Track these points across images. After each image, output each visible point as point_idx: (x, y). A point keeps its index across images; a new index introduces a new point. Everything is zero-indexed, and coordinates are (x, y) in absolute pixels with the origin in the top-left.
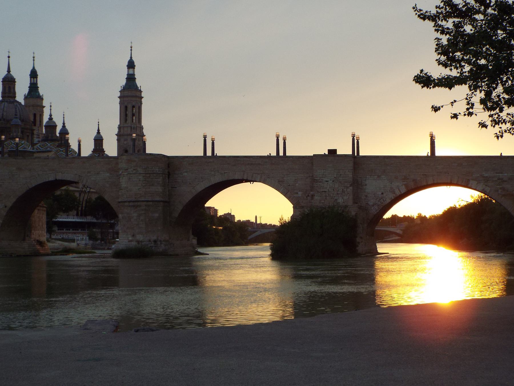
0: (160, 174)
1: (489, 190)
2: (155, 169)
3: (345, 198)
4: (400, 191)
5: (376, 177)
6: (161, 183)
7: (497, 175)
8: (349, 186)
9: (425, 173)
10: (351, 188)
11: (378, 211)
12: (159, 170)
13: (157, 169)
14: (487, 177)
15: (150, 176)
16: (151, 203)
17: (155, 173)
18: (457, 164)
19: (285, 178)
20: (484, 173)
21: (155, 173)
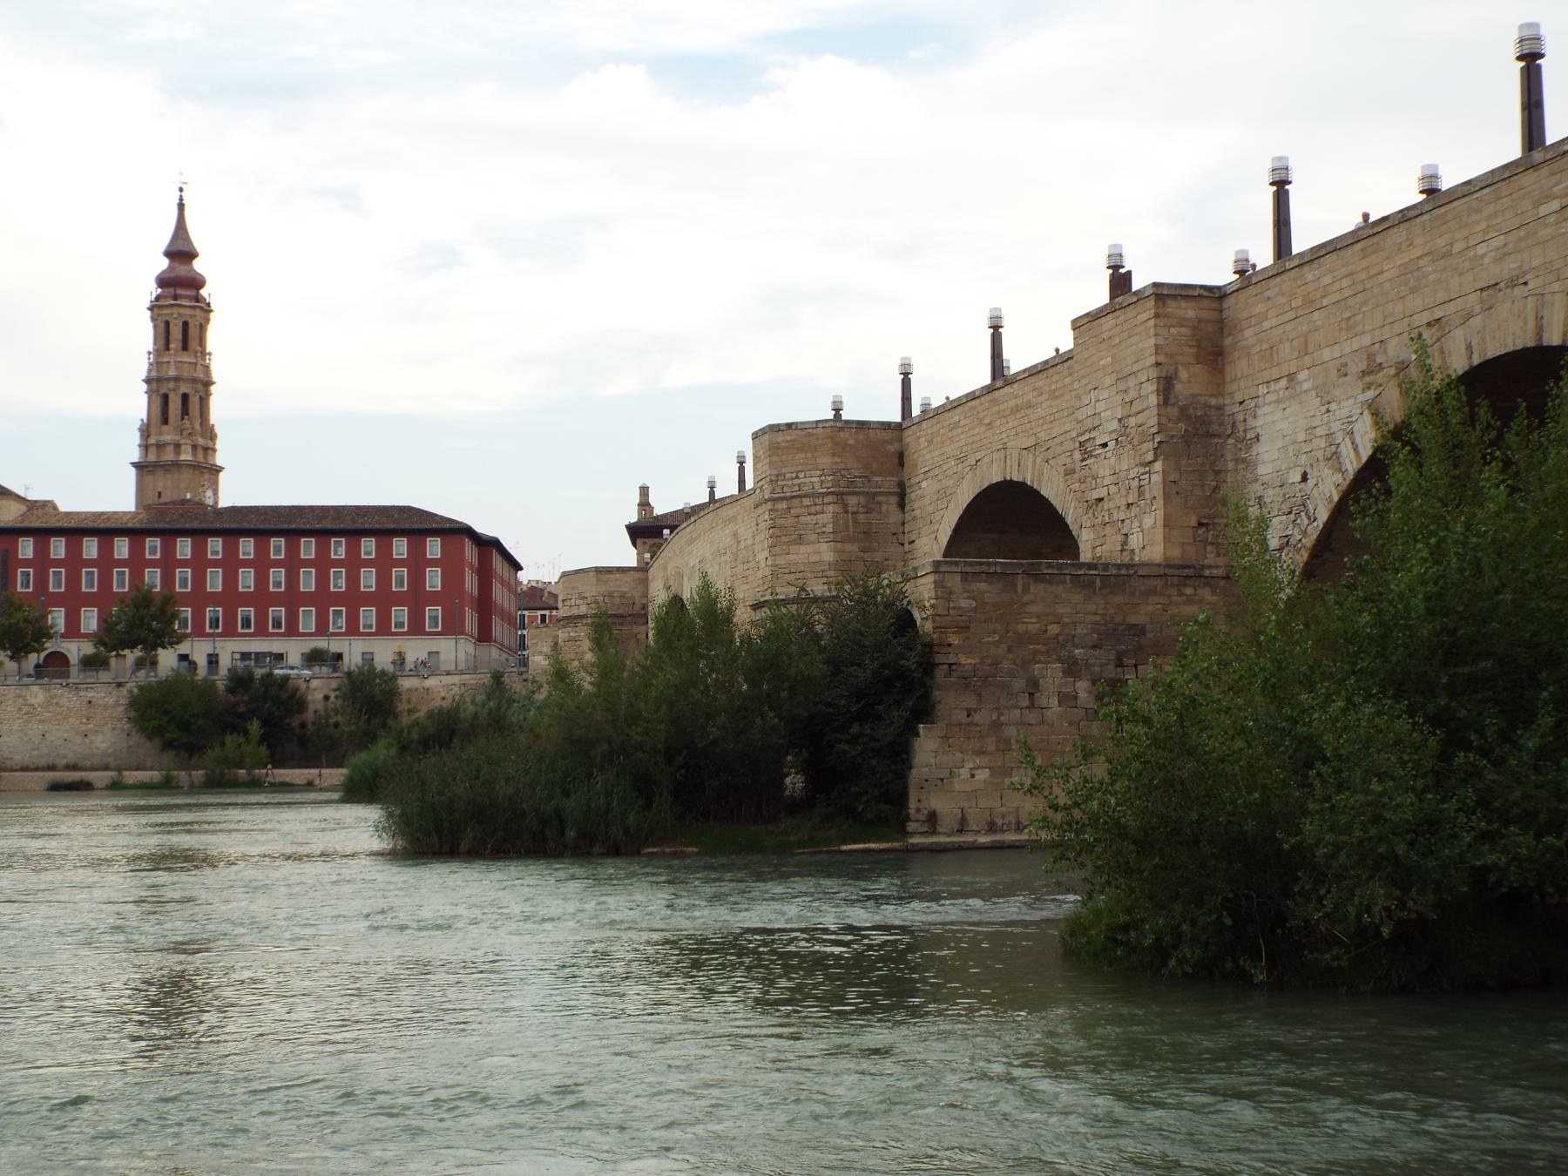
2: (807, 480)
3: (1148, 521)
4: (1356, 449)
5: (1283, 383)
6: (830, 528)
8: (1150, 457)
9: (1438, 314)
12: (822, 482)
13: (813, 479)
17: (805, 496)
21: (805, 496)
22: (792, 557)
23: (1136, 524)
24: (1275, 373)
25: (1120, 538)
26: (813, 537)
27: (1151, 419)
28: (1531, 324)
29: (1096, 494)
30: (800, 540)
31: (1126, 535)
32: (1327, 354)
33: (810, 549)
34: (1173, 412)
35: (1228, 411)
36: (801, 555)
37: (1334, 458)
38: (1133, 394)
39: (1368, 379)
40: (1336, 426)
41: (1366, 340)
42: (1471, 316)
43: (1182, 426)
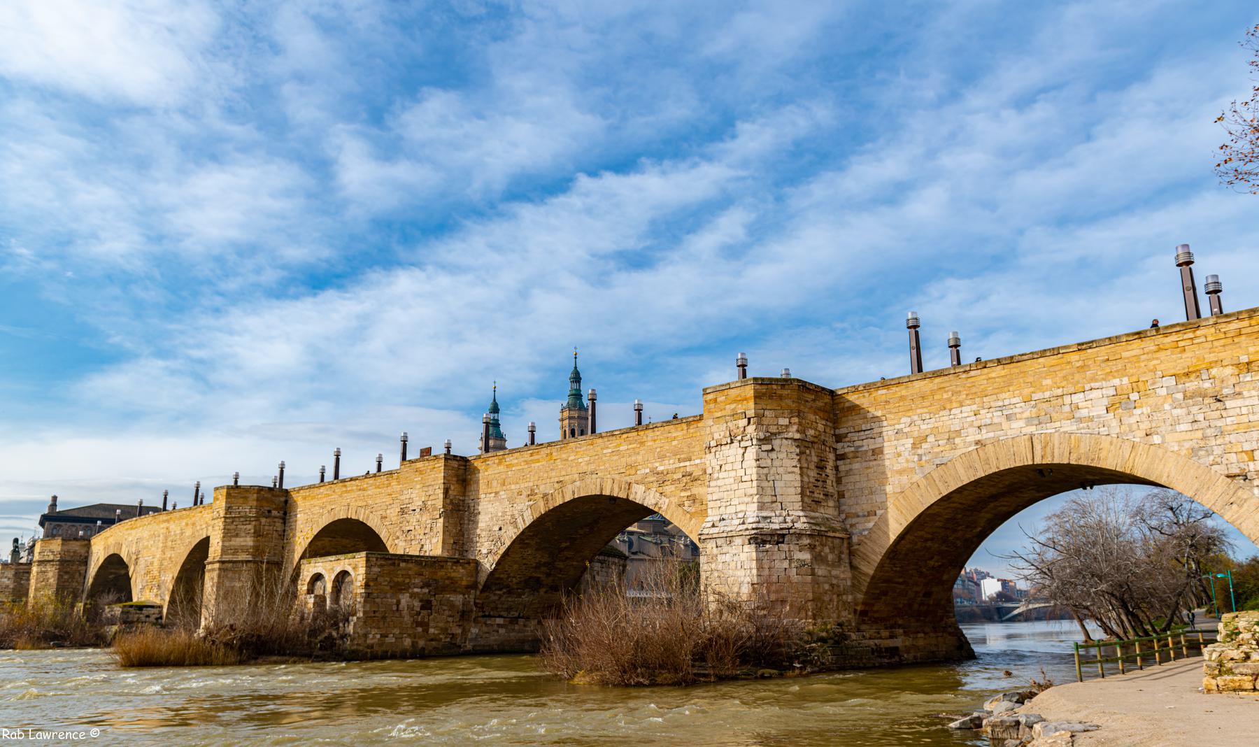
0: (251, 517)
1: (666, 504)
3: (434, 540)
4: (524, 521)
5: (493, 495)
6: (252, 531)
7: (682, 464)
8: (438, 516)
10: (441, 520)
11: (493, 567)
14: (662, 473)
15: (233, 522)
16: (230, 565)
18: (610, 451)
19: (388, 511)
20: (657, 464)
22: (232, 543)
23: (428, 541)
24: (489, 490)
25: (420, 546)
26: (243, 534)
27: (440, 503)
28: (598, 487)
29: (408, 528)
30: (237, 535)
31: (423, 545)
32: (513, 487)
33: (242, 539)
34: (448, 501)
35: (466, 502)
36: (237, 542)
37: (514, 523)
38: (431, 492)
39: (530, 497)
40: (516, 512)
41: (531, 484)
42: (575, 481)
43: (451, 506)
